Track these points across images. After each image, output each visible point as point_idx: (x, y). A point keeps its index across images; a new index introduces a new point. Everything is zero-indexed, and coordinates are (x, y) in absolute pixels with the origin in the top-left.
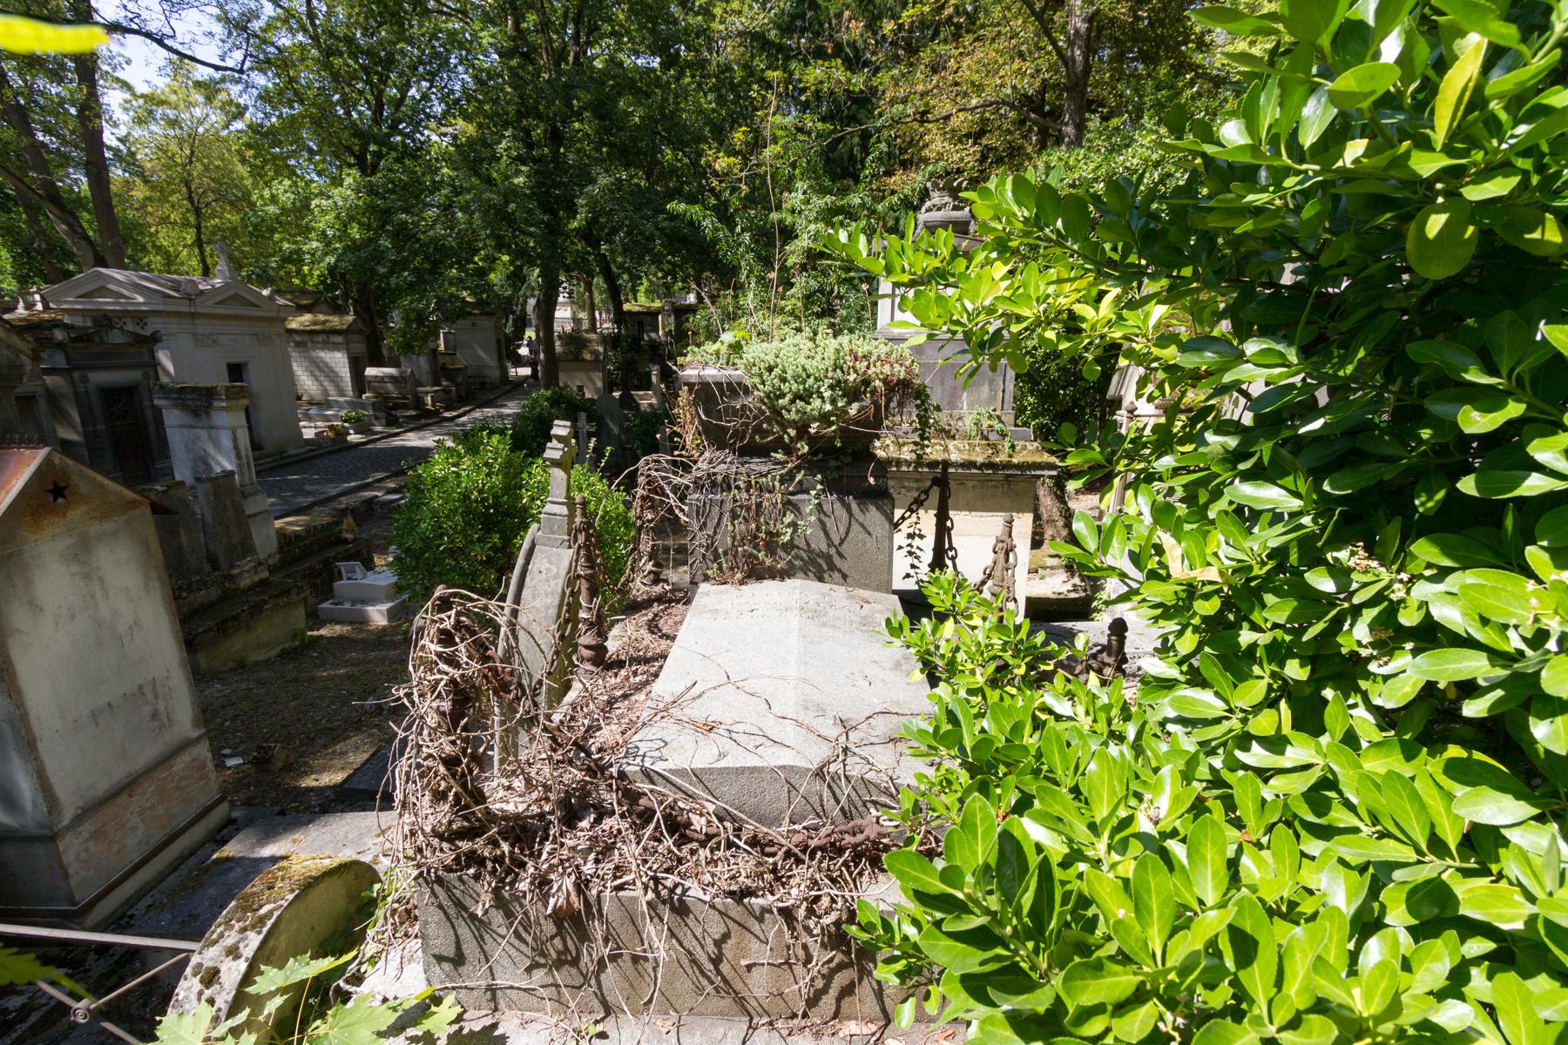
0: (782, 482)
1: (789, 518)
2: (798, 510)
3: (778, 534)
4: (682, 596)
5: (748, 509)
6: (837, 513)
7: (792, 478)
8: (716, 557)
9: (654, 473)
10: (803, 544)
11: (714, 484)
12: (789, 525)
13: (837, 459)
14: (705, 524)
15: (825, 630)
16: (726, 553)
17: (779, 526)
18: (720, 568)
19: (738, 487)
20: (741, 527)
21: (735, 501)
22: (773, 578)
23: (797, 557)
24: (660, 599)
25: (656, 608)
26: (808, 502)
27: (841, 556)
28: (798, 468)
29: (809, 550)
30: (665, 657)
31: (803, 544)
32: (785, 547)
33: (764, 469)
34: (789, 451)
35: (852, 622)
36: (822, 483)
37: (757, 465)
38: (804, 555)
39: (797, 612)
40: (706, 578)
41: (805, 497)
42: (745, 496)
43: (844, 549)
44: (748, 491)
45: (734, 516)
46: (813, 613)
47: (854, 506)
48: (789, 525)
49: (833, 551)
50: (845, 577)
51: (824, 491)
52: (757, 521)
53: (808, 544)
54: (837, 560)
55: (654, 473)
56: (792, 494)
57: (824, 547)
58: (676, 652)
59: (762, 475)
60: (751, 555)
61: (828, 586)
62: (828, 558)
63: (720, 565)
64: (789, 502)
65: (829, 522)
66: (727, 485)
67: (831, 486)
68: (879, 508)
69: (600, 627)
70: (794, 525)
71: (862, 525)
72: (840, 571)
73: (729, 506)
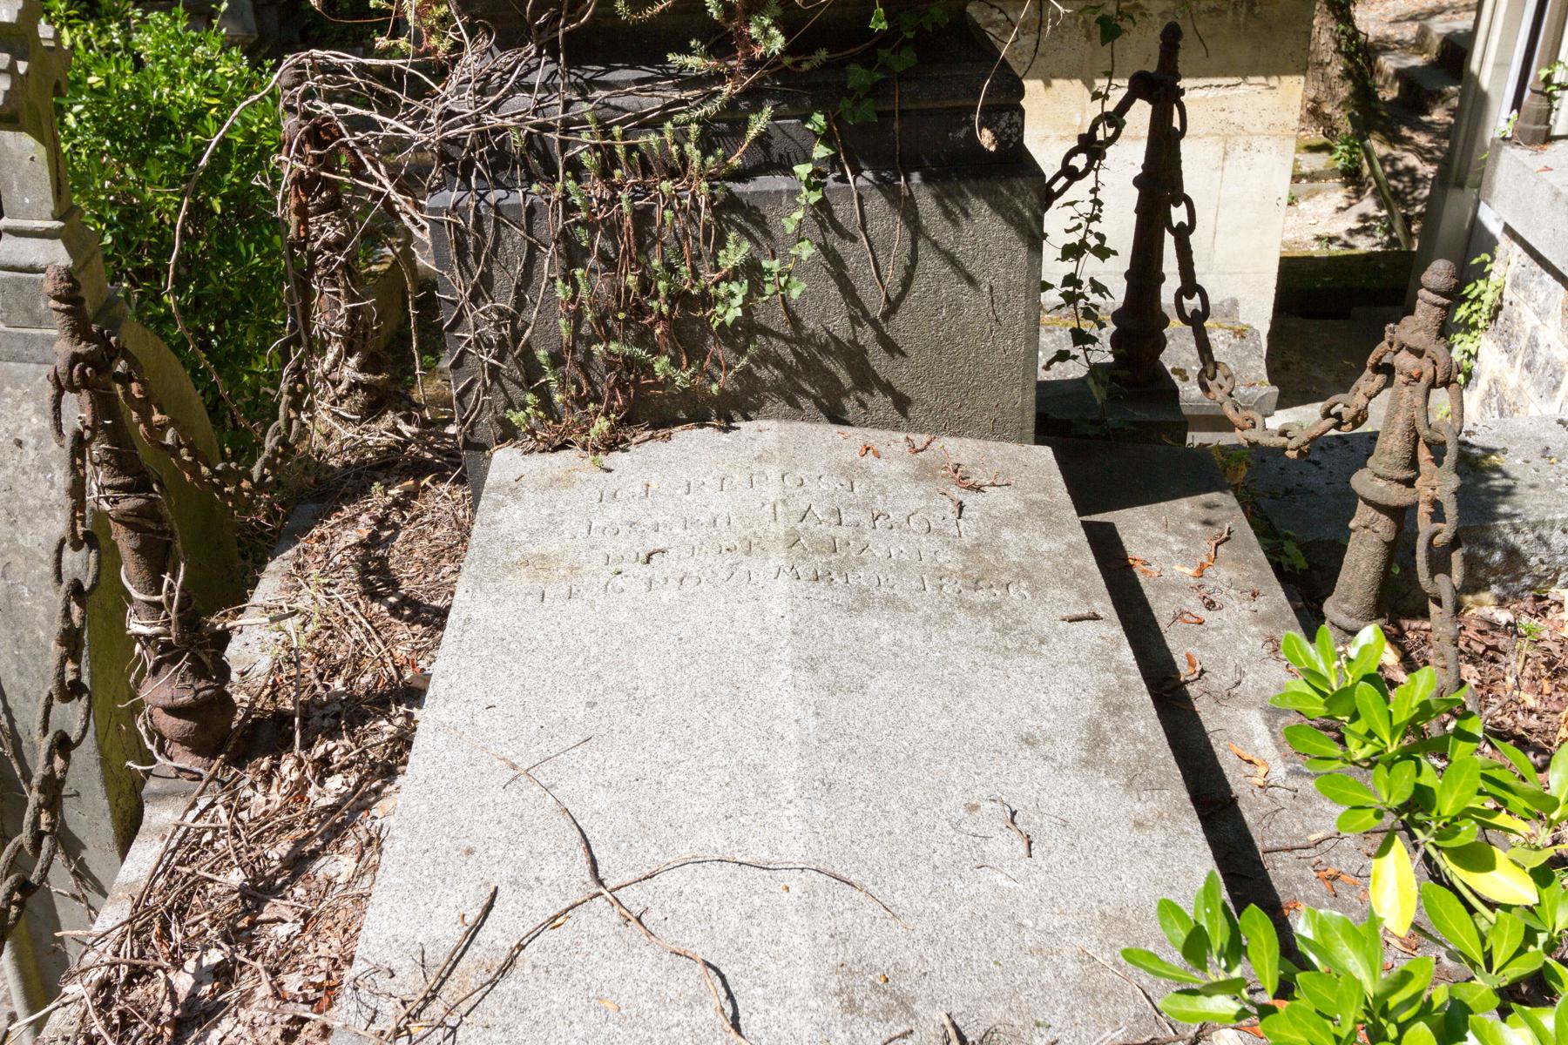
0: (706, 147)
1: (735, 254)
2: (761, 222)
3: (707, 300)
4: (459, 464)
5: (613, 229)
6: (875, 227)
7: (738, 127)
8: (531, 373)
9: (326, 109)
10: (779, 322)
11: (501, 160)
12: (734, 275)
13: (868, 61)
14: (487, 280)
15: (869, 622)
16: (556, 360)
17: (708, 277)
18: (546, 403)
19: (575, 166)
20: (593, 284)
21: (570, 208)
22: (701, 420)
23: (764, 358)
24: (390, 465)
25: (380, 496)
26: (790, 198)
27: (890, 346)
28: (755, 97)
29: (798, 334)
30: (414, 694)
31: (779, 322)
32: (729, 335)
33: (650, 103)
34: (721, 42)
35: (940, 574)
36: (827, 139)
37: (630, 90)
38: (786, 352)
39: (778, 558)
40: (508, 434)
41: (778, 182)
42: (597, 189)
43: (899, 327)
44: (605, 173)
45: (573, 255)
46: (824, 556)
47: (926, 202)
48: (734, 275)
49: (866, 336)
50: (902, 403)
51: (833, 161)
52: (643, 267)
53: (794, 320)
54: (879, 361)
55: (326, 109)
56: (741, 175)
57: (840, 325)
58: (452, 668)
59: (647, 123)
60: (630, 363)
61: (855, 436)
62: (854, 356)
63: (544, 395)
64: (733, 203)
65: (854, 256)
66: (538, 159)
67: (853, 148)
68: (997, 207)
69: (200, 648)
70: (751, 271)
71: (950, 259)
72: (887, 388)
73: (551, 225)
